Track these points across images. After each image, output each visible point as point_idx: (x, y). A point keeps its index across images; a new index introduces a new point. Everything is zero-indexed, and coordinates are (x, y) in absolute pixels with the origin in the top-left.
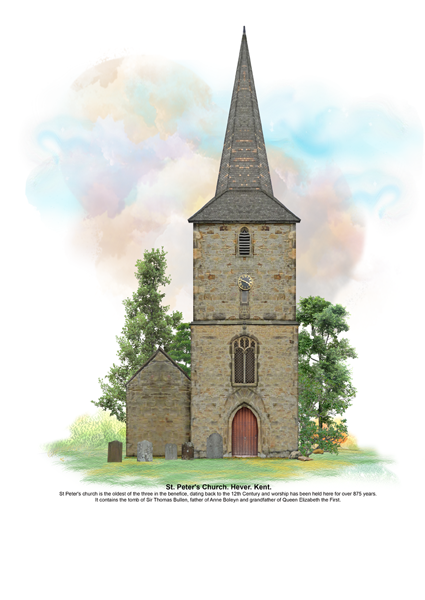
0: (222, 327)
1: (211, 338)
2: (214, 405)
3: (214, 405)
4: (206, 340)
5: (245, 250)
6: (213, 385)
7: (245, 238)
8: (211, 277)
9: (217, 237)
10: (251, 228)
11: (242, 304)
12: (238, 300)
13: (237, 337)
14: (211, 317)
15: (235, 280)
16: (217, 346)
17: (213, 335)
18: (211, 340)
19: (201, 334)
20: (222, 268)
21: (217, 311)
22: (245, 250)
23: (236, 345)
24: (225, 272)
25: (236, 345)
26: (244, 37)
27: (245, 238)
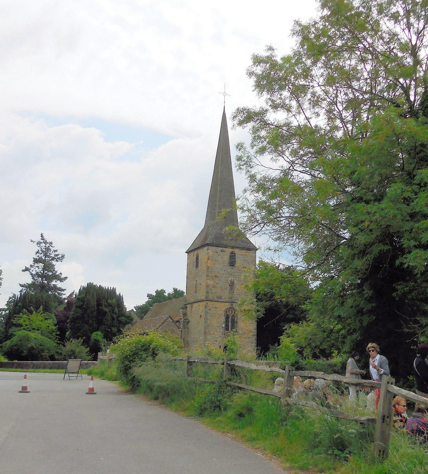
1: (216, 308)
2: (216, 341)
3: (216, 341)
4: (213, 309)
5: (232, 263)
6: (216, 331)
7: (233, 256)
8: (216, 276)
10: (236, 251)
12: (228, 289)
13: (227, 309)
14: (216, 299)
16: (219, 312)
17: (217, 306)
18: (216, 309)
22: (232, 263)
23: (226, 312)
24: (223, 274)
25: (226, 312)
26: (224, 111)
27: (233, 256)
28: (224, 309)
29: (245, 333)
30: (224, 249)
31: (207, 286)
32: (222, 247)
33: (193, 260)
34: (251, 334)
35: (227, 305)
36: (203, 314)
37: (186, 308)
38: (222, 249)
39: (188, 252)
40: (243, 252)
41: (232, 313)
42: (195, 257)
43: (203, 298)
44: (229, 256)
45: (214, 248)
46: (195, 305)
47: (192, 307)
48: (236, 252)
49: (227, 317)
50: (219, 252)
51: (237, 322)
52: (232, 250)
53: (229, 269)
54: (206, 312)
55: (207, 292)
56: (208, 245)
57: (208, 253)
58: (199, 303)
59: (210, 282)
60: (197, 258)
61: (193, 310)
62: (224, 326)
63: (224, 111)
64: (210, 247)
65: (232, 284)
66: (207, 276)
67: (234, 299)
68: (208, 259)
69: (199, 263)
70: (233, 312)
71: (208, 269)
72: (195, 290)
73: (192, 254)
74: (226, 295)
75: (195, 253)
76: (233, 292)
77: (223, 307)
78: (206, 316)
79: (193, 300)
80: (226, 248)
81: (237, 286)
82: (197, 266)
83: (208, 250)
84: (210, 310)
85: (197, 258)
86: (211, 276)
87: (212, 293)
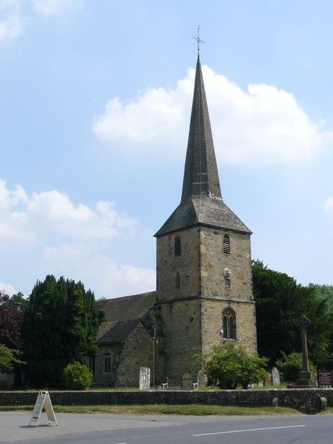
5: (226, 251)
8: (211, 266)
10: (230, 234)
26: (198, 60)
28: (221, 309)
33: (169, 245)
35: (226, 305)
37: (160, 308)
39: (158, 235)
42: (173, 241)
46: (178, 305)
47: (172, 307)
58: (187, 302)
60: (178, 241)
61: (173, 311)
62: (222, 331)
63: (198, 60)
65: (227, 277)
73: (166, 238)
74: (221, 289)
75: (173, 236)
77: (222, 306)
81: (233, 279)
82: (178, 251)
85: (178, 241)
86: (205, 266)
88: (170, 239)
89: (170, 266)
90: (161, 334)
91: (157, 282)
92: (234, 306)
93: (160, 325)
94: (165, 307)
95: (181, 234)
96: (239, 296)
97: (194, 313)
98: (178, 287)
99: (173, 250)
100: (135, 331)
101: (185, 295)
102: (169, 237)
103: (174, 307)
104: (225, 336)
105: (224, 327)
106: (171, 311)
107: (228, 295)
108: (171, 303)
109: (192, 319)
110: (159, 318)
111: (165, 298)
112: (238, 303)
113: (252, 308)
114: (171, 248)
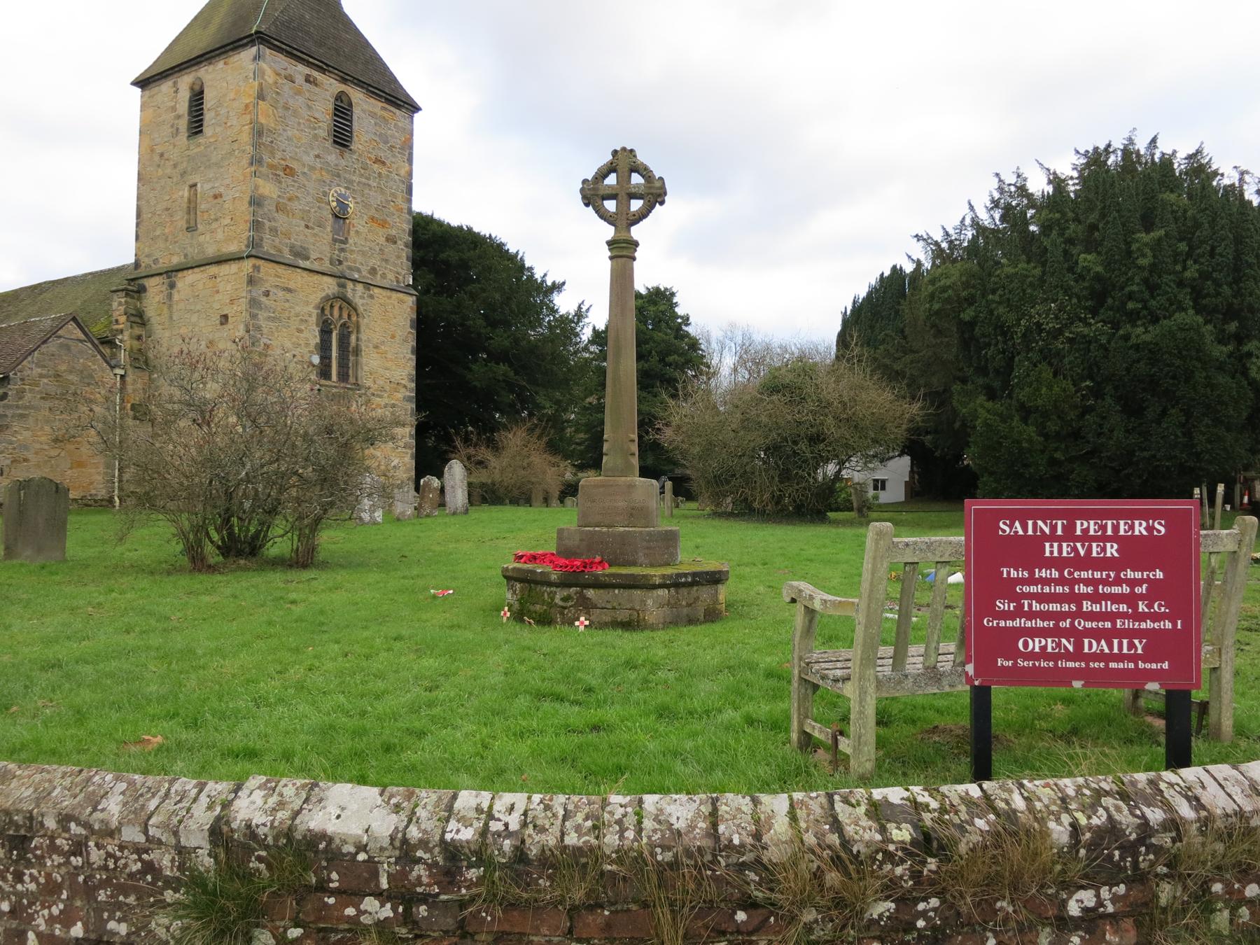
0: (305, 274)
1: (289, 290)
4: (281, 294)
5: (342, 137)
7: (342, 111)
9: (299, 93)
10: (357, 96)
11: (335, 240)
12: (329, 229)
13: (327, 299)
14: (288, 257)
15: (325, 194)
16: (298, 309)
17: (292, 285)
18: (288, 296)
19: (272, 280)
20: (306, 159)
21: (296, 240)
22: (342, 137)
23: (323, 310)
24: (312, 168)
25: (323, 310)
27: (342, 111)
28: (316, 298)
29: (383, 389)
30: (316, 74)
31: (256, 202)
32: (309, 64)
33: (174, 109)
34: (400, 396)
35: (329, 286)
36: (238, 312)
37: (142, 290)
38: (307, 70)
39: (143, 83)
40: (376, 106)
41: (340, 316)
43: (233, 248)
44: (331, 107)
45: (282, 61)
46: (190, 277)
48: (354, 101)
49: (325, 332)
50: (300, 80)
51: (357, 351)
52: (343, 87)
53: (332, 156)
54: (253, 303)
55: (256, 225)
56: (259, 38)
57: (258, 74)
58: (213, 270)
59: (268, 189)
60: (197, 98)
61: (176, 297)
62: (316, 360)
64: (268, 51)
65: (340, 216)
66: (256, 161)
67: (350, 268)
68: (261, 96)
69: (208, 117)
70: (345, 316)
71: (259, 132)
72: (188, 222)
73: (166, 87)
74: (320, 247)
75: (185, 82)
76: (345, 242)
78: (254, 316)
79: (176, 260)
80: (323, 71)
81: (358, 222)
82: (196, 126)
83: (257, 57)
84: (267, 294)
85: (197, 98)
86: (271, 166)
87: (274, 231)
88: (176, 92)
89: (175, 166)
90: (141, 361)
91: (139, 215)
92: (356, 293)
93: (139, 338)
94: (154, 287)
95: (216, 77)
96: (373, 271)
97: (232, 301)
98: (191, 228)
99: (183, 124)
100: (52, 346)
101: (211, 251)
102: (175, 83)
103: (180, 285)
104: (325, 372)
105: (324, 348)
106: (170, 296)
107: (340, 263)
108: (171, 273)
109: (225, 319)
110: (138, 318)
111: (156, 261)
112: (368, 285)
113: (410, 301)
114: (179, 117)
